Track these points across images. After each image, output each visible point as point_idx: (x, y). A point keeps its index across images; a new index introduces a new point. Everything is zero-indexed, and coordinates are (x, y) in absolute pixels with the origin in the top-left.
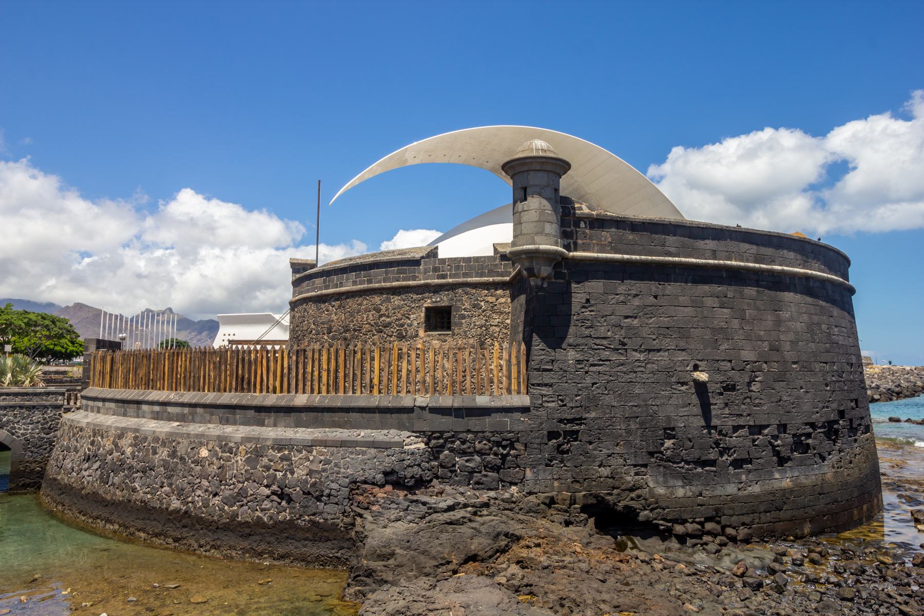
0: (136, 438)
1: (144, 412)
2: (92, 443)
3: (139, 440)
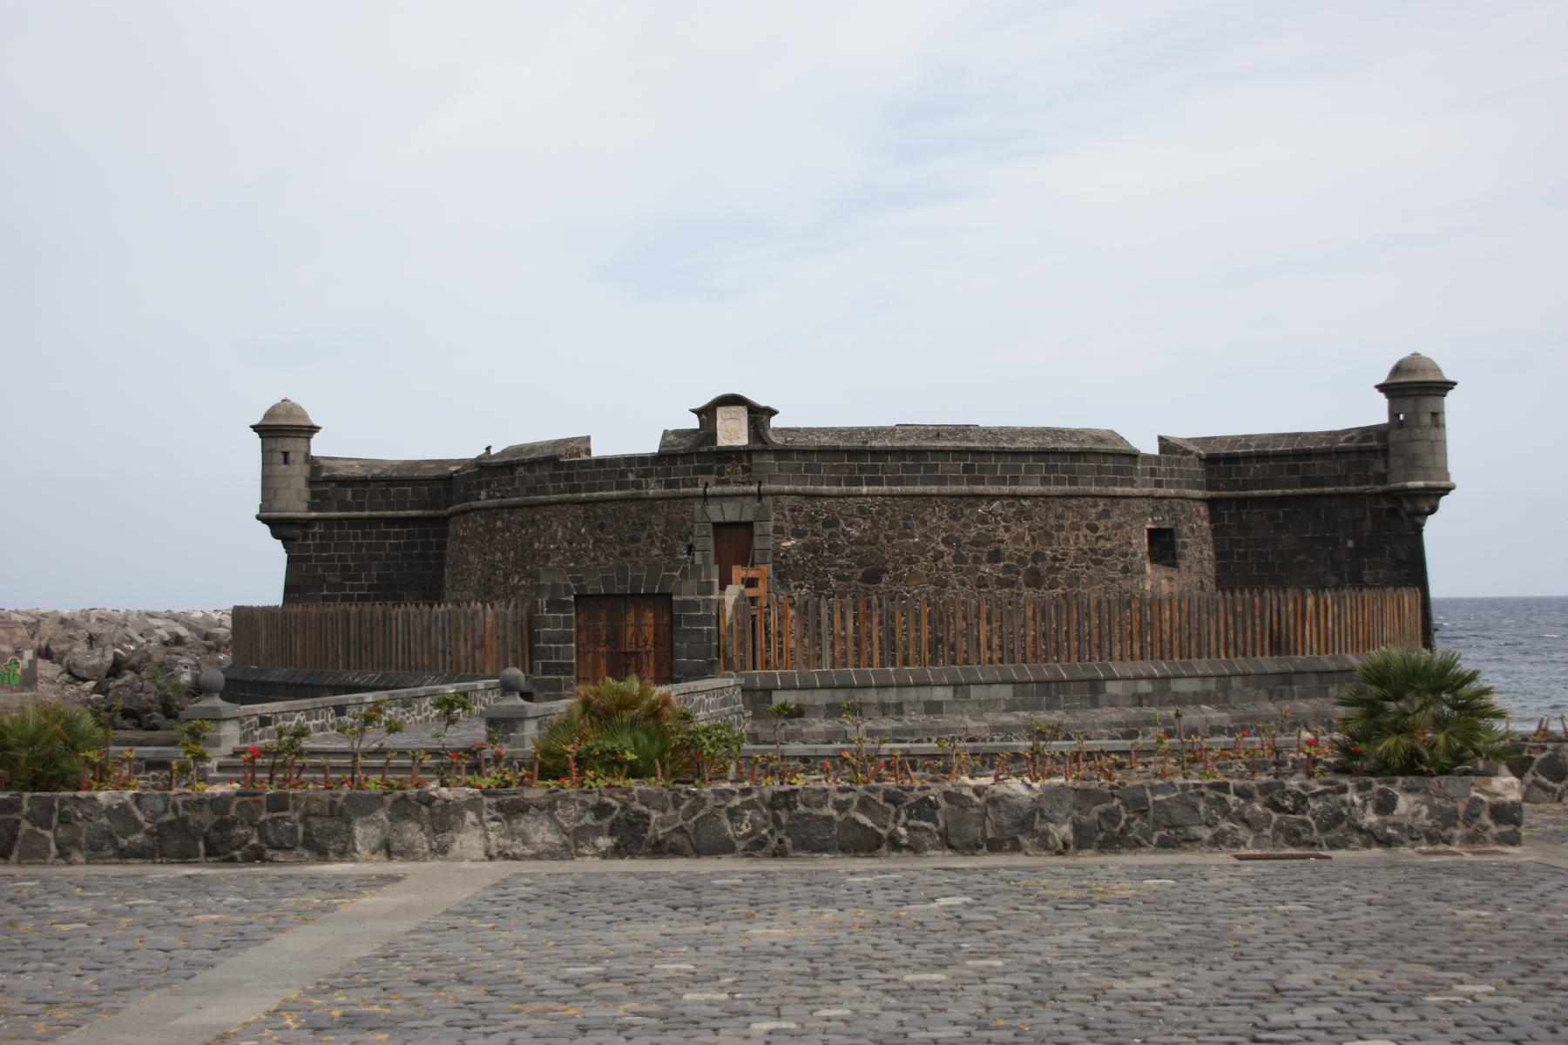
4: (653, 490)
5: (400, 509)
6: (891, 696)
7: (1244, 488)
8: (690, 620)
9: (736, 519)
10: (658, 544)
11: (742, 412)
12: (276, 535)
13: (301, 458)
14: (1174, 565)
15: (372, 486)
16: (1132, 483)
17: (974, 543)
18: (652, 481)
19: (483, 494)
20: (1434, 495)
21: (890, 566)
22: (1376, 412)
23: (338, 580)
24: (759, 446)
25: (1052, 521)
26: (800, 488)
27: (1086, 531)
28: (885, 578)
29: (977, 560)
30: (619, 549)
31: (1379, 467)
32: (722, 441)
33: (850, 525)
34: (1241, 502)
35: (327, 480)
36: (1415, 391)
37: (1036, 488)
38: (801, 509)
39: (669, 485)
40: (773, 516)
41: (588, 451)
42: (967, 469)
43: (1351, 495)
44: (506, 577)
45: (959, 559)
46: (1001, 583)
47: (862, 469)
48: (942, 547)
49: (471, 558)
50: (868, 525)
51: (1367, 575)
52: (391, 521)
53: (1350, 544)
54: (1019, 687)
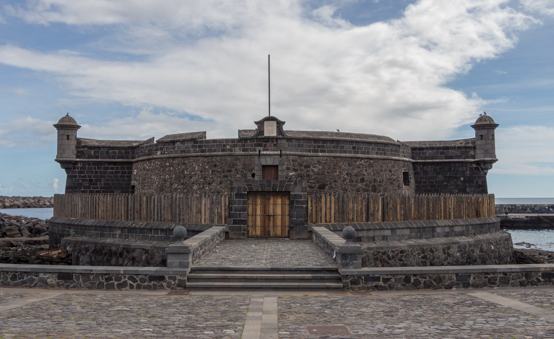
0: (459, 247)
1: (439, 233)
2: (425, 257)
3: (461, 248)
4: (238, 151)
5: (113, 158)
6: (371, 234)
7: (425, 159)
8: (298, 202)
9: (272, 164)
10: (239, 173)
11: (275, 123)
12: (62, 167)
13: (74, 138)
14: (409, 185)
15: (102, 149)
16: (398, 156)
17: (356, 175)
18: (237, 149)
19: (159, 153)
20: (488, 164)
21: (328, 183)
22: (471, 134)
23: (88, 185)
24: (281, 136)
25: (379, 168)
26: (297, 153)
27: (388, 172)
28: (327, 187)
29: (357, 181)
30: (223, 174)
31: (472, 153)
32: (266, 134)
33: (314, 167)
34: (424, 164)
35: (84, 147)
36: (485, 127)
37: (375, 156)
38: (296, 161)
39: (244, 150)
40: (286, 163)
41: (205, 137)
42: (354, 148)
43: (462, 162)
44: (171, 185)
45: (351, 181)
46: (365, 190)
47: (318, 147)
48: (346, 177)
49: (153, 177)
50: (321, 167)
51: (468, 190)
52: (110, 163)
53: (462, 179)
54: (411, 230)
